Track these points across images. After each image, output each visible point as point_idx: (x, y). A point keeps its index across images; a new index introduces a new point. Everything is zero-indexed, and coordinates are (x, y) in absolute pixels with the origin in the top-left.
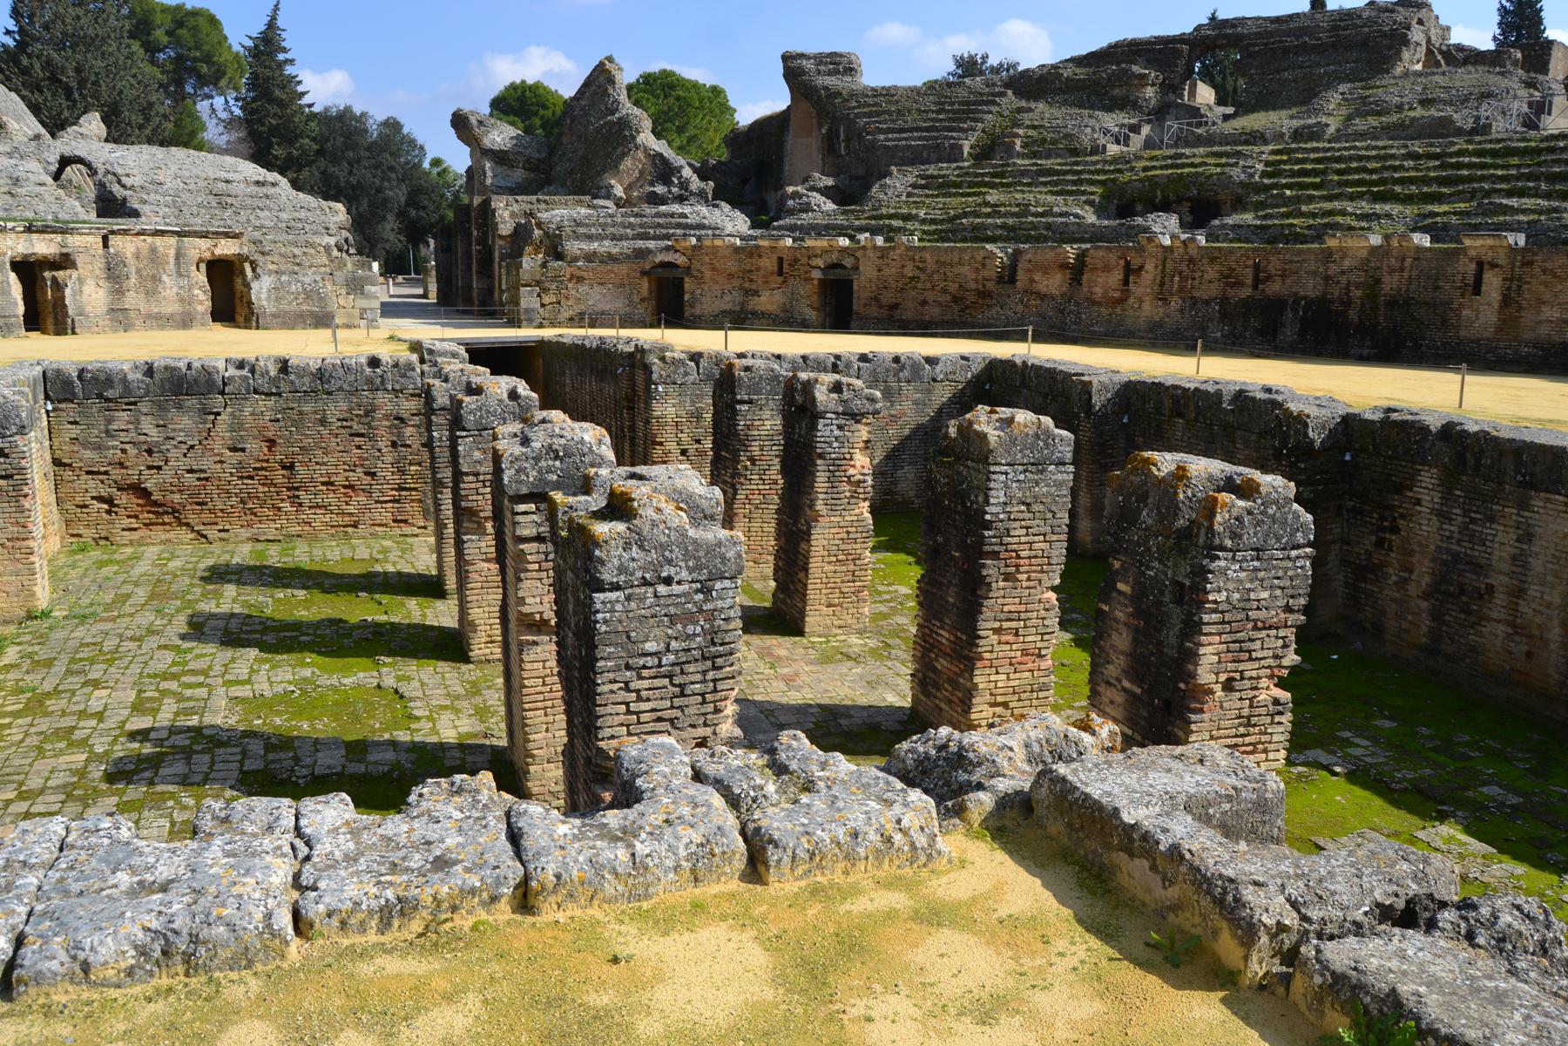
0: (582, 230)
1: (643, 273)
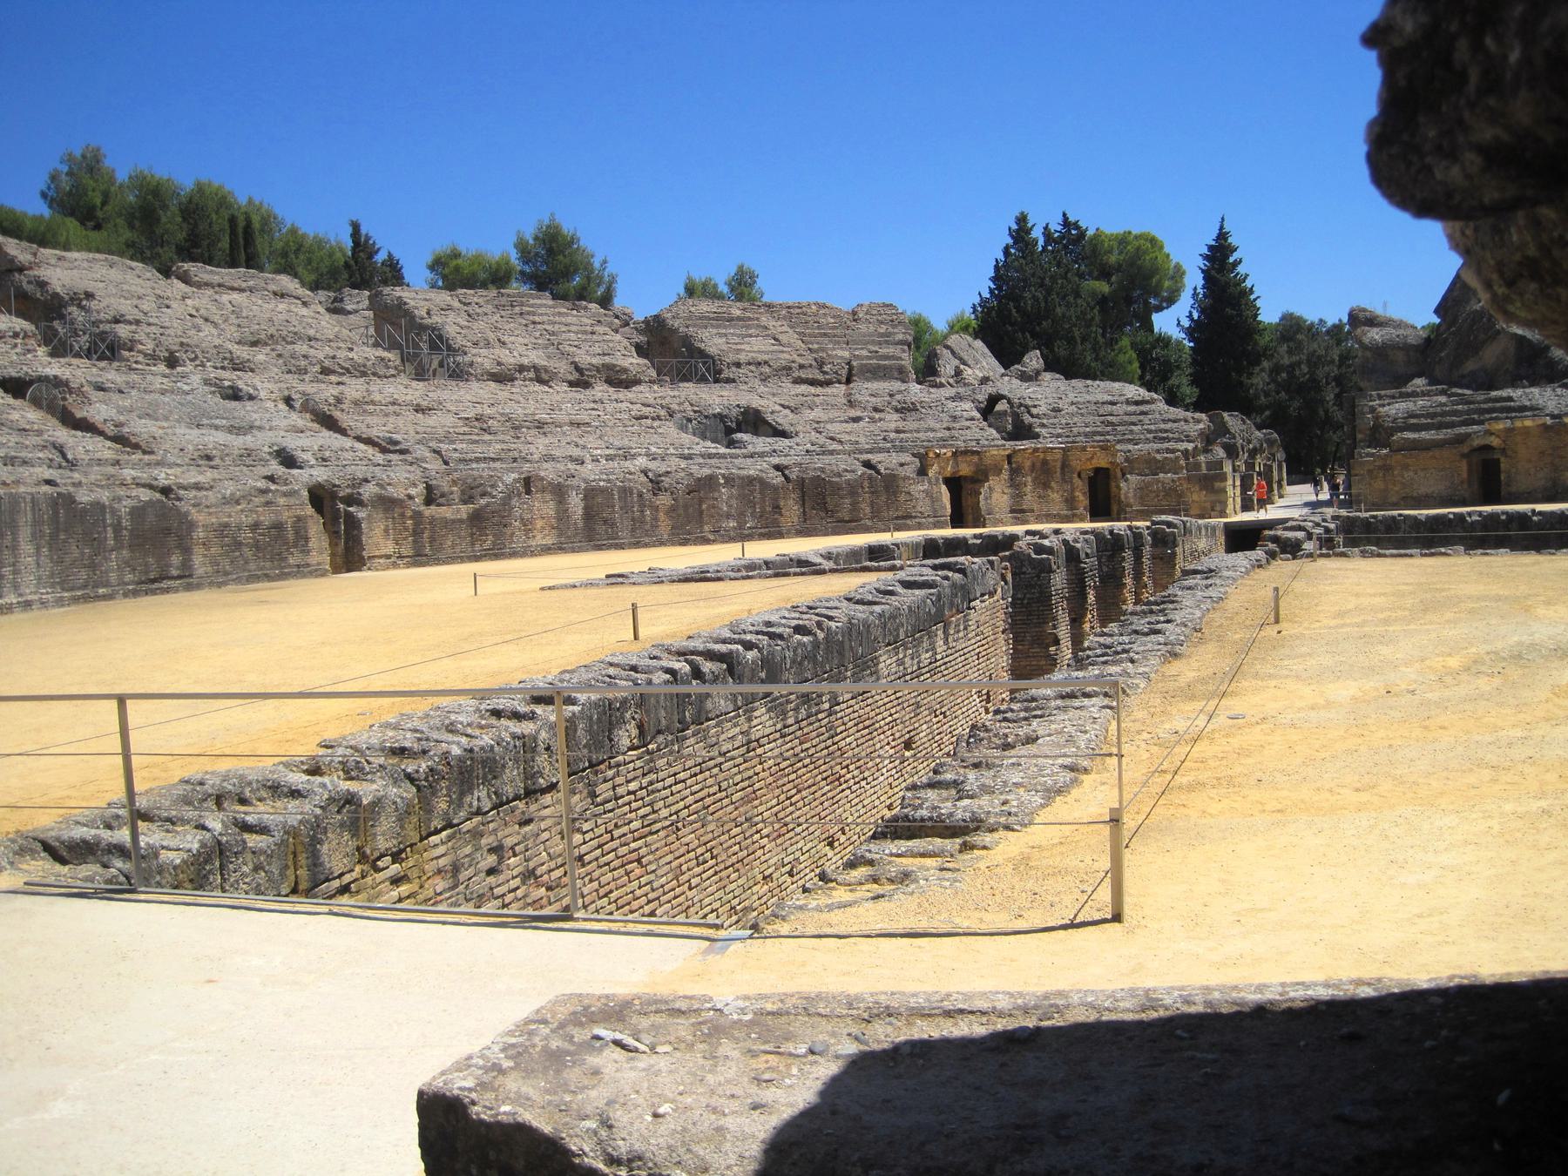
0: (1413, 421)
1: (1463, 456)
